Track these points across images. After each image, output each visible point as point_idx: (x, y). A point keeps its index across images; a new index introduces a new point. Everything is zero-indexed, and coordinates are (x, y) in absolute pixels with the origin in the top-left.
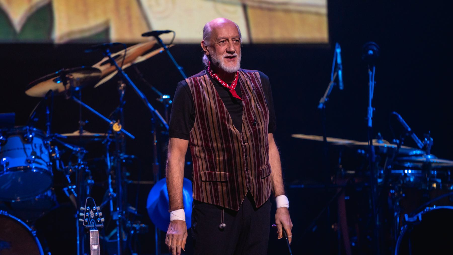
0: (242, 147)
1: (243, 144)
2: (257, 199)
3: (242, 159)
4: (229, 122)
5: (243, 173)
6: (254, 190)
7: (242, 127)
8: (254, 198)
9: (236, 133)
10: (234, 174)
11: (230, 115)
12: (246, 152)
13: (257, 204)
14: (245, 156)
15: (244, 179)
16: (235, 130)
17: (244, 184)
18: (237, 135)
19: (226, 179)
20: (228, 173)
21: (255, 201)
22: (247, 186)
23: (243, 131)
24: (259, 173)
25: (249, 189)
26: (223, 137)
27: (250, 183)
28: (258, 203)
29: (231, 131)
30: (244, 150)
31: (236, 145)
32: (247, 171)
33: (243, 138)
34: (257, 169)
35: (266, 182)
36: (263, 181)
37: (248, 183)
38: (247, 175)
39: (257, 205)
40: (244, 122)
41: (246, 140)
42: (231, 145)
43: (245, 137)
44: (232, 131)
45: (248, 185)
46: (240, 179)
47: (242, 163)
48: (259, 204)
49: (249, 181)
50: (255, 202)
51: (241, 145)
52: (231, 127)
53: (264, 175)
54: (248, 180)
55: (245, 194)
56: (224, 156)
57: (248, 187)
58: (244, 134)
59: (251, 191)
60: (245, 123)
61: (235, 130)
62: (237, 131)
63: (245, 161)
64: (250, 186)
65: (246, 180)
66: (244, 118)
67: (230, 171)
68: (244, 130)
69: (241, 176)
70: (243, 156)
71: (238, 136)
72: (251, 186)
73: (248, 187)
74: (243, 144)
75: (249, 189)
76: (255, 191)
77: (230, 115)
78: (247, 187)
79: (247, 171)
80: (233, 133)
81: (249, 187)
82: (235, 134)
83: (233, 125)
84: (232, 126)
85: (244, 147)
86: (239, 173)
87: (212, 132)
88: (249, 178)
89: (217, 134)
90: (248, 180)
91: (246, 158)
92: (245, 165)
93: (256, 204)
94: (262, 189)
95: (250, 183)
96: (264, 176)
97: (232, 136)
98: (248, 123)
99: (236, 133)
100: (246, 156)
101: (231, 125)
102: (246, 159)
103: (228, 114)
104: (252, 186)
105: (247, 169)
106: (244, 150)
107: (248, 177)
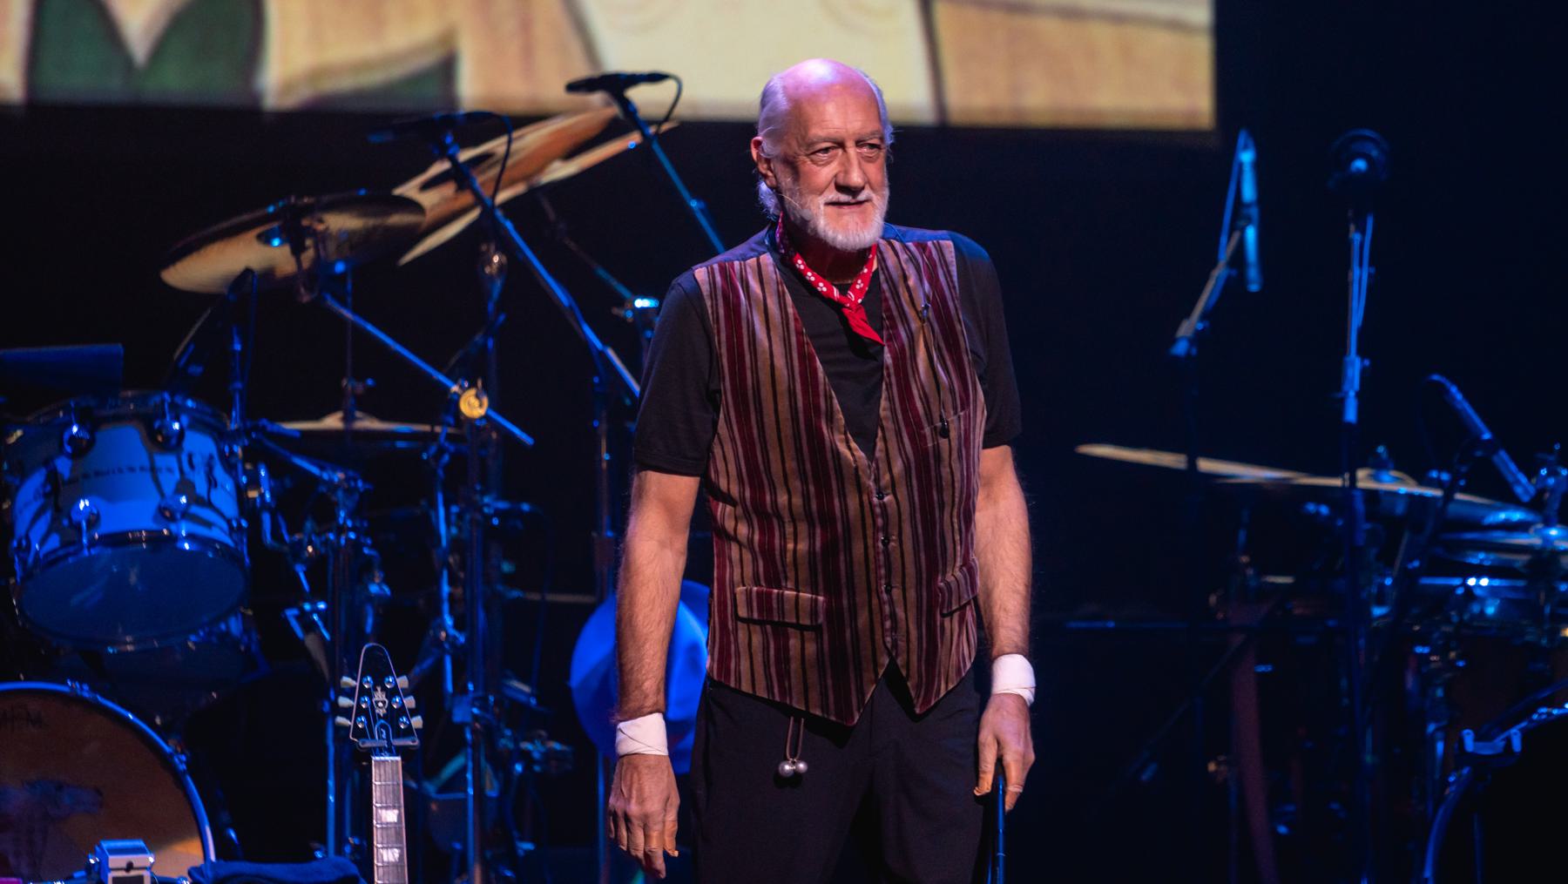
1: (875, 500)
2: (918, 687)
4: (832, 422)
5: (875, 601)
7: (878, 440)
8: (909, 684)
9: (855, 461)
10: (845, 602)
11: (835, 401)
12: (886, 524)
14: (883, 541)
15: (877, 619)
16: (850, 451)
18: (857, 469)
20: (824, 596)
22: (884, 643)
25: (894, 654)
26: (810, 474)
27: (896, 632)
29: (837, 454)
30: (880, 521)
31: (853, 503)
32: (888, 592)
37: (888, 633)
40: (884, 423)
42: (836, 501)
45: (888, 639)
46: (863, 619)
47: (872, 566)
49: (894, 628)
51: (870, 503)
52: (841, 440)
54: (888, 624)
56: (812, 536)
57: (889, 645)
58: (883, 466)
59: (900, 661)
60: (889, 425)
61: (850, 451)
62: (860, 454)
63: (882, 557)
64: (895, 644)
65: (883, 625)
67: (833, 592)
68: (881, 451)
69: (867, 609)
70: (875, 540)
71: (860, 473)
72: (899, 643)
73: (889, 645)
74: (875, 500)
75: (894, 654)
76: (914, 658)
77: (835, 401)
79: (888, 592)
81: (892, 646)
82: (850, 464)
83: (845, 434)
84: (843, 437)
85: (878, 510)
86: (861, 597)
87: (774, 456)
88: (893, 616)
89: (791, 464)
90: (888, 624)
92: (883, 571)
95: (896, 632)
100: (885, 544)
101: (840, 433)
102: (887, 553)
103: (831, 397)
104: (902, 644)
105: (888, 584)
106: (880, 521)
107: (891, 612)
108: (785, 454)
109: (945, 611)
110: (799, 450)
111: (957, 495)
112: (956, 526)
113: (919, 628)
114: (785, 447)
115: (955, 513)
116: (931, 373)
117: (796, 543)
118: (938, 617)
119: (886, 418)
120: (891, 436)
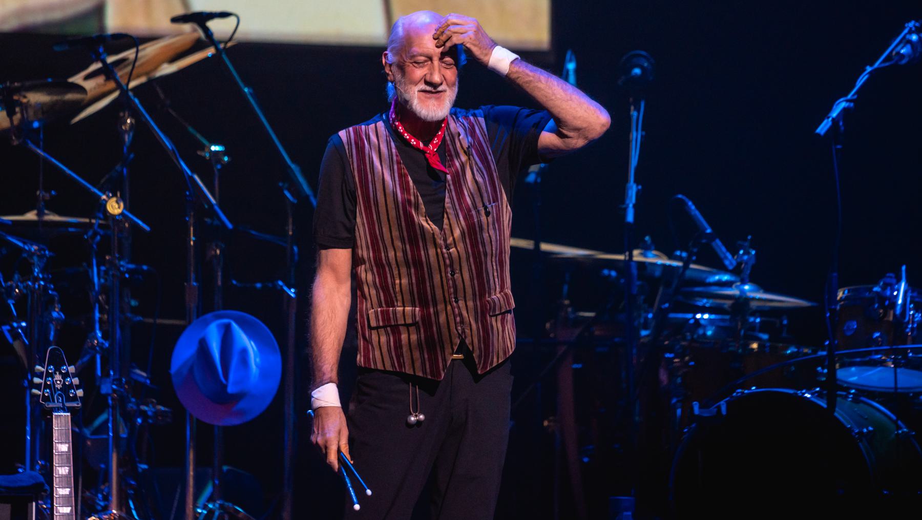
0: (443, 257)
1: (444, 250)
2: (480, 357)
3: (444, 279)
4: (418, 210)
5: (449, 308)
6: (473, 339)
7: (445, 219)
8: (474, 355)
9: (432, 230)
10: (432, 310)
11: (420, 198)
12: (452, 265)
13: (479, 367)
14: (451, 274)
15: (451, 318)
16: (428, 226)
17: (451, 328)
18: (433, 234)
19: (415, 319)
20: (420, 307)
21: (477, 361)
22: (457, 330)
23: (446, 226)
24: (483, 306)
25: (463, 337)
26: (406, 238)
27: (463, 324)
28: (481, 365)
29: (422, 227)
30: (448, 262)
31: (432, 252)
32: (457, 302)
33: (445, 240)
34: (478, 297)
35: (499, 325)
36: (494, 323)
37: (459, 325)
38: (456, 310)
39: (480, 368)
40: (448, 210)
41: (453, 242)
42: (422, 253)
43: (450, 237)
44: (425, 228)
45: (459, 328)
46: (442, 318)
47: (446, 288)
48: (485, 367)
49: (462, 322)
50: (477, 363)
51: (442, 252)
52: (424, 220)
53: (494, 310)
54: (458, 319)
55: (454, 347)
56: (409, 275)
57: (460, 332)
58: (448, 232)
59: (468, 341)
60: (450, 211)
61: (428, 226)
62: (434, 226)
63: (451, 282)
64: (464, 331)
65: (455, 320)
66: (447, 203)
67: (424, 304)
68: (446, 224)
69: (445, 312)
70: (446, 273)
71: (436, 236)
72: (466, 330)
73: (460, 332)
74: (444, 250)
75: (463, 337)
76: (476, 341)
77: (420, 198)
78: (458, 332)
79: (457, 302)
80: (425, 230)
81: (462, 333)
82: (430, 232)
83: (425, 217)
84: (424, 218)
85: (446, 255)
86: (441, 307)
87: (385, 230)
88: (461, 315)
89: (396, 233)
90: (458, 319)
91: (454, 278)
92: (452, 290)
93: (478, 366)
94: (491, 337)
95: (463, 324)
96: (495, 312)
97: (424, 235)
98: (457, 211)
99: (432, 230)
100: (453, 275)
101: (422, 216)
102: (454, 281)
103: (417, 196)
104: (467, 331)
105: (456, 298)
106: (448, 262)
107: (459, 313)
108: (392, 228)
109: (491, 314)
110: (400, 225)
111: (494, 249)
112: (495, 267)
113: (477, 322)
114: (392, 224)
115: (494, 260)
116: (474, 181)
117: (400, 279)
118: (488, 318)
119: (449, 208)
120: (452, 217)
